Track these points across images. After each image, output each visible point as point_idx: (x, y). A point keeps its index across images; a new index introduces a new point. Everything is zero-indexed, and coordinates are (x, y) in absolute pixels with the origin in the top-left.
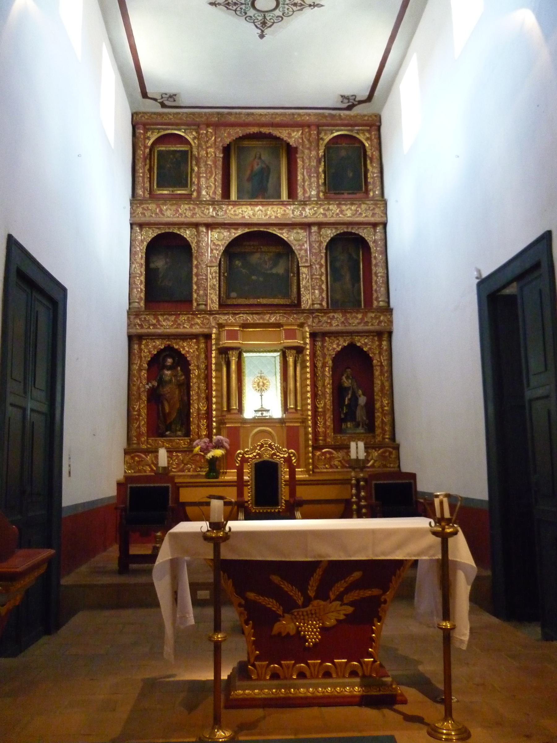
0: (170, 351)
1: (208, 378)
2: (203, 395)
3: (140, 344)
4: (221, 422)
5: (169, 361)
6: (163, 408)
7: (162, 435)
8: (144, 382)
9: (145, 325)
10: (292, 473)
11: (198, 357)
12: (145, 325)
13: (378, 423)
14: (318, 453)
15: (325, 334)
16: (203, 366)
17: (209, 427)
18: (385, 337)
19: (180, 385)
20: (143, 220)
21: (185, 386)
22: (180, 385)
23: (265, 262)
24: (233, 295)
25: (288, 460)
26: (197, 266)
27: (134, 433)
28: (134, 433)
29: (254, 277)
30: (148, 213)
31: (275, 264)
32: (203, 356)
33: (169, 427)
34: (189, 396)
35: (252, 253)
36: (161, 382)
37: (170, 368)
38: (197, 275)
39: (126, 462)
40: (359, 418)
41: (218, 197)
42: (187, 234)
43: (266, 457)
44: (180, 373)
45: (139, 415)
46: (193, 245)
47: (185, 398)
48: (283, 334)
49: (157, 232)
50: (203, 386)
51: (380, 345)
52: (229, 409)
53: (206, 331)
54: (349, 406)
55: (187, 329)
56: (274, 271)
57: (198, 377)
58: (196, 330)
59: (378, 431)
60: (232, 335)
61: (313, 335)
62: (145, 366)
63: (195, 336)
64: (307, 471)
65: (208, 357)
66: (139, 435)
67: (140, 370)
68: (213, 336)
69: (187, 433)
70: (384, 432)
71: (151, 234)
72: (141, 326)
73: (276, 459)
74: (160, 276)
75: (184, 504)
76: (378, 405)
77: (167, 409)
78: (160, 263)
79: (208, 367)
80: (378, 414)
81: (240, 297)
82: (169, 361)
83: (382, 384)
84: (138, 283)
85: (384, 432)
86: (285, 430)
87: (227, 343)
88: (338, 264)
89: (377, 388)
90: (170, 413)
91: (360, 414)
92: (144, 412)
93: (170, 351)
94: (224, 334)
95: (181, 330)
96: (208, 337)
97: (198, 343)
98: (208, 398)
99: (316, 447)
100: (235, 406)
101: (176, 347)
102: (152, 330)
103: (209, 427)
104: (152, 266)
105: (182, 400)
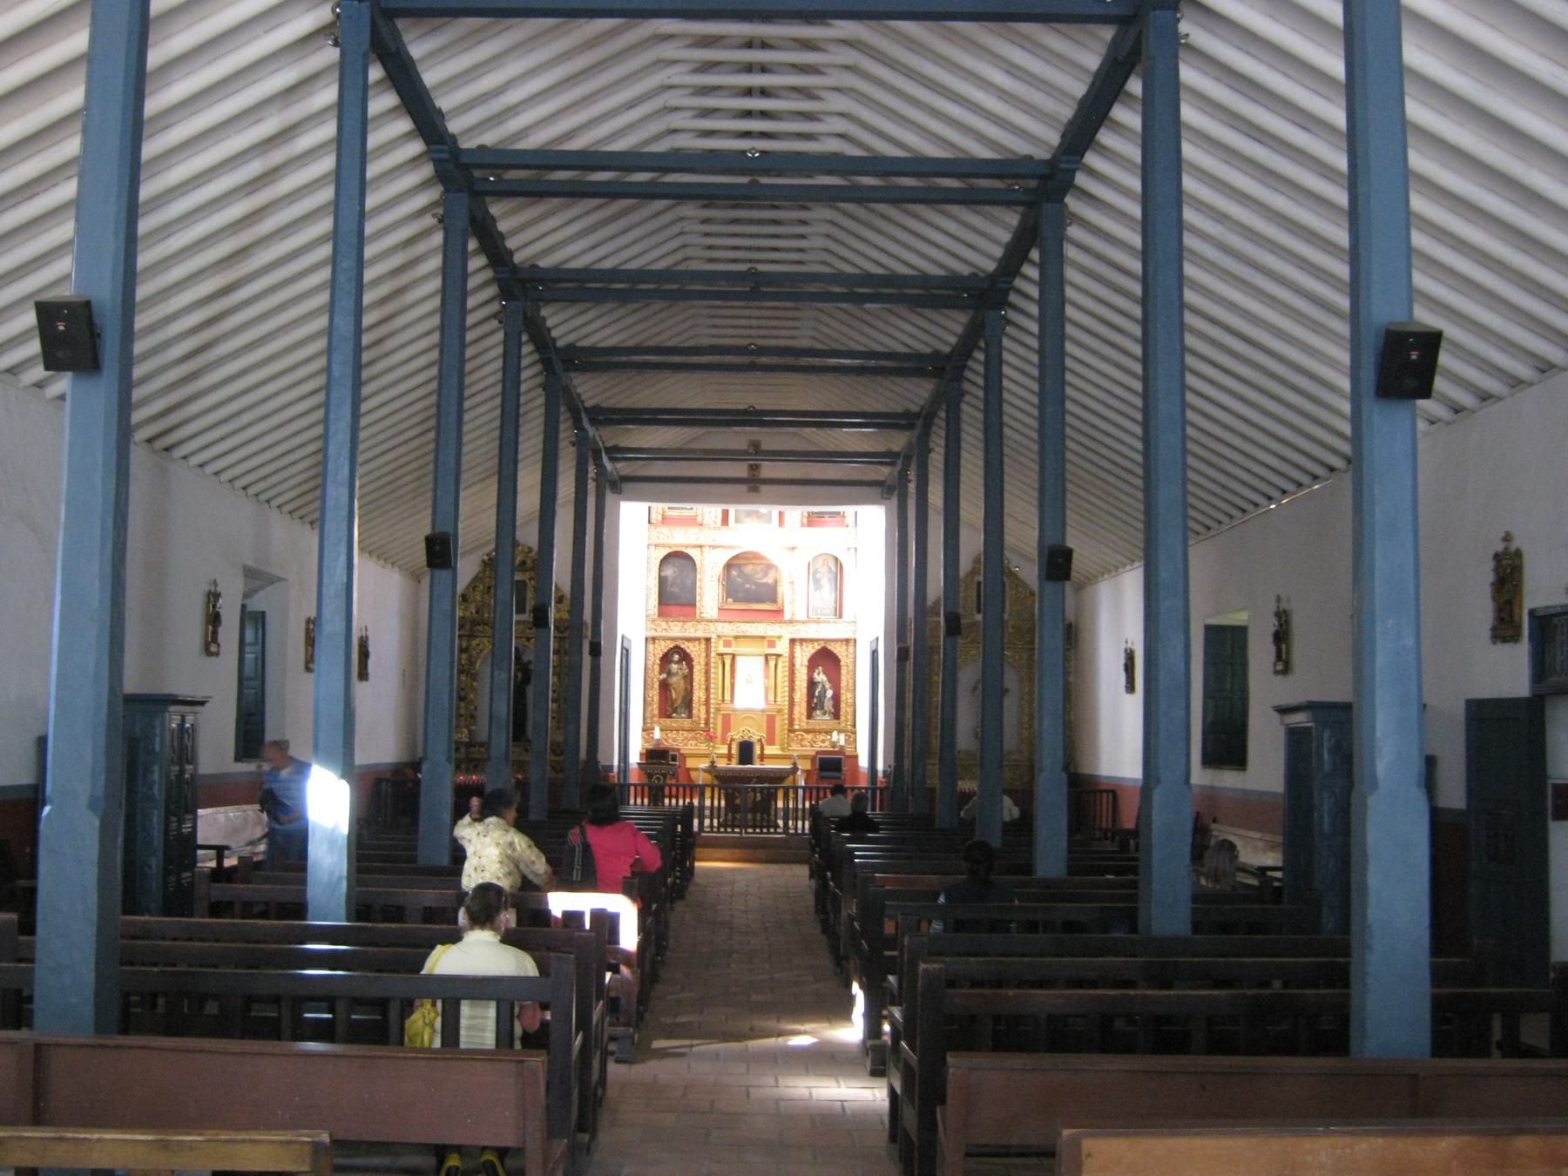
0: (677, 649)
1: (707, 672)
2: (704, 687)
3: (654, 643)
4: (718, 710)
5: (676, 657)
6: (671, 695)
7: (670, 717)
8: (657, 673)
9: (659, 629)
10: (762, 749)
11: (699, 657)
12: (659, 629)
13: (842, 712)
14: (792, 735)
15: (802, 641)
16: (703, 663)
17: (708, 712)
18: (851, 643)
19: (685, 677)
20: (658, 542)
21: (689, 678)
22: (685, 677)
23: (757, 573)
24: (730, 600)
25: (760, 740)
26: (700, 580)
27: (648, 715)
28: (648, 715)
29: (747, 586)
30: (661, 536)
31: (766, 575)
32: (704, 654)
33: (675, 711)
34: (692, 686)
35: (746, 564)
36: (670, 674)
37: (677, 663)
38: (700, 588)
39: (643, 738)
40: (826, 708)
41: (719, 521)
42: (692, 552)
43: (746, 738)
44: (685, 666)
45: (653, 700)
46: (698, 563)
47: (689, 687)
48: (766, 643)
49: (669, 550)
50: (703, 679)
51: (847, 650)
52: (723, 700)
53: (707, 635)
54: (819, 697)
55: (691, 633)
56: (764, 580)
57: (700, 671)
58: (700, 634)
59: (842, 718)
60: (728, 644)
61: (793, 641)
62: (658, 661)
63: (698, 639)
64: (782, 749)
65: (708, 656)
66: (654, 716)
67: (654, 664)
68: (713, 640)
69: (690, 716)
70: (847, 720)
71: (664, 552)
72: (656, 630)
73: (752, 740)
74: (669, 583)
75: (688, 769)
76: (843, 698)
77: (674, 696)
78: (669, 572)
79: (707, 664)
80: (843, 705)
81: (735, 601)
82: (676, 657)
83: (848, 682)
84: (652, 592)
85: (847, 720)
86: (765, 718)
87: (722, 649)
88: (818, 576)
89: (843, 684)
90: (676, 700)
91: (828, 705)
92: (656, 698)
93: (677, 649)
94: (721, 642)
95: (687, 634)
96: (708, 640)
97: (700, 643)
98: (707, 689)
99: (791, 730)
100: (727, 697)
101: (682, 646)
102: (664, 634)
103: (708, 712)
104: (662, 574)
105: (686, 690)
